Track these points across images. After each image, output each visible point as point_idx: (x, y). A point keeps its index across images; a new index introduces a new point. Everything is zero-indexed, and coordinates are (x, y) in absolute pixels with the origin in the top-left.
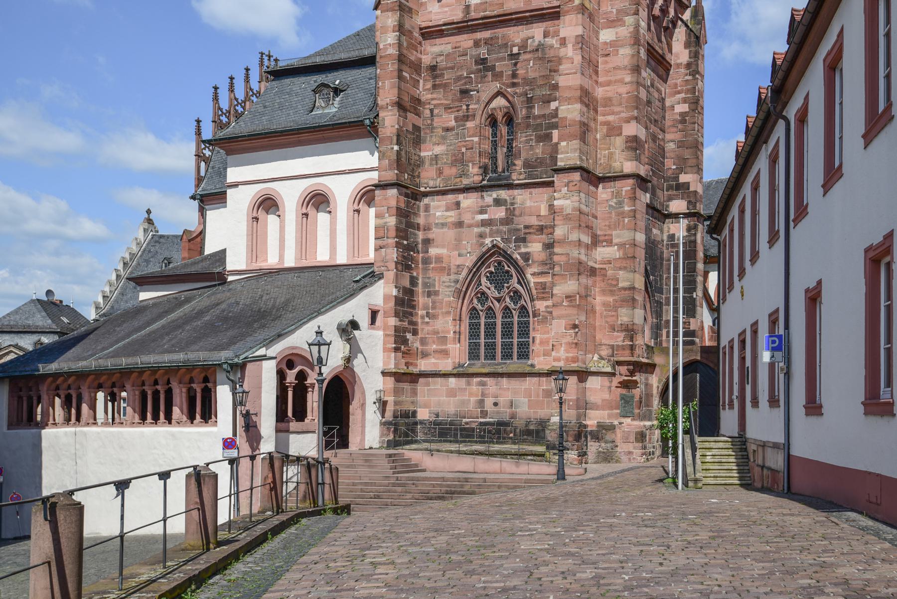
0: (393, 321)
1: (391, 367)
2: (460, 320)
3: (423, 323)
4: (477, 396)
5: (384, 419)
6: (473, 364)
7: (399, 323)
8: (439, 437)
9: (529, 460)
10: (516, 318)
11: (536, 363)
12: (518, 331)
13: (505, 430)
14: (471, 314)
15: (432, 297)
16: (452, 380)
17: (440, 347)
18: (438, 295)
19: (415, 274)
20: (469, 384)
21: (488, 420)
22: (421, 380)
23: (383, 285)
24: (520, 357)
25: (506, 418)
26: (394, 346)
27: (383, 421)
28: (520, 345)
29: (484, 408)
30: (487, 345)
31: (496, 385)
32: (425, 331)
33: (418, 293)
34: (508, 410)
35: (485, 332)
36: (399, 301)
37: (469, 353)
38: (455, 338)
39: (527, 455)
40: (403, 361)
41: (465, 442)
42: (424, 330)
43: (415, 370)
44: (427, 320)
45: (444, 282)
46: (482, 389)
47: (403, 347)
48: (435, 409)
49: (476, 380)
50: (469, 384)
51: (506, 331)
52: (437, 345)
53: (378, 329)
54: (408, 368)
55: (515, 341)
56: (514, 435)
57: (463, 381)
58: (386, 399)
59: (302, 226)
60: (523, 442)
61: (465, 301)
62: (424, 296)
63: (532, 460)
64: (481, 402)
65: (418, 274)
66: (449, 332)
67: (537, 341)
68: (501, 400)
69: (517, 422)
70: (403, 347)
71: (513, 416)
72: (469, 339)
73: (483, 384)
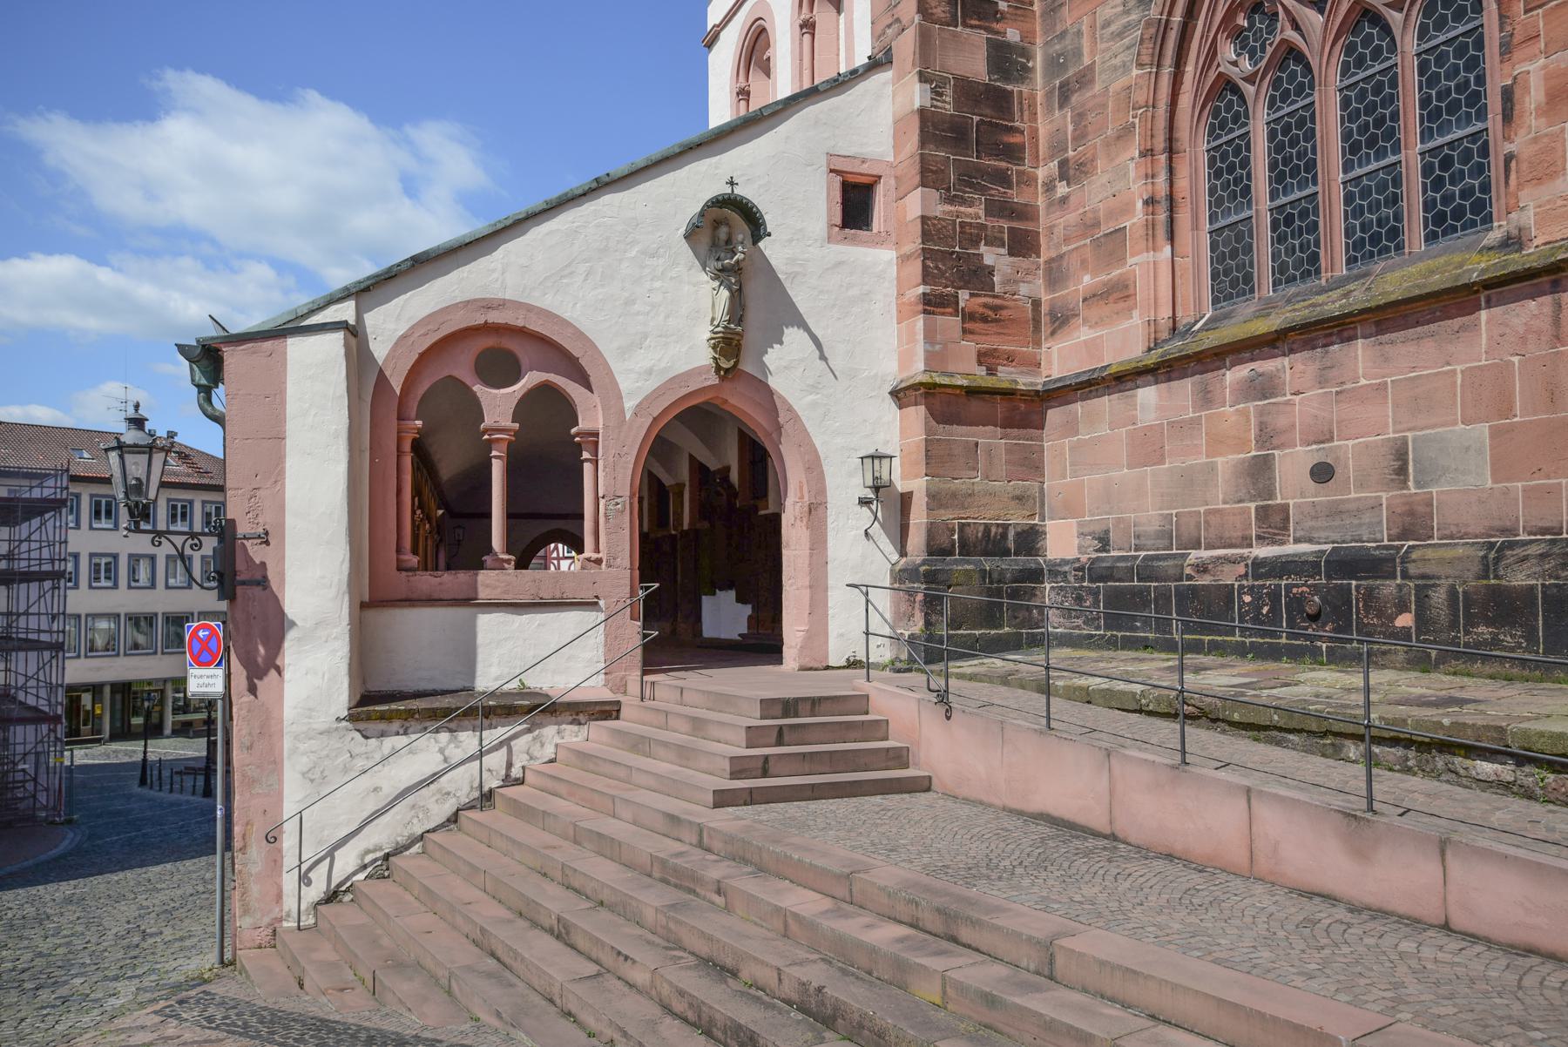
0: (915, 204)
1: (917, 370)
2: (1171, 150)
3: (1050, 205)
4: (1242, 445)
5: (904, 560)
6: (1227, 316)
7: (940, 210)
8: (1107, 628)
9: (1485, 784)
10: (1410, 44)
11: (1528, 218)
12: (1425, 102)
13: (1369, 596)
14: (1216, 113)
15: (1075, 99)
16: (1148, 395)
17: (1104, 277)
18: (1092, 81)
19: (1013, 35)
20: (1206, 398)
21: (1290, 549)
22: (1054, 416)
23: (890, 89)
24: (1441, 223)
25: (1376, 535)
26: (921, 289)
27: (898, 568)
28: (1439, 167)
29: (1271, 496)
30: (1284, 221)
31: (1322, 382)
32: (1059, 232)
33: (1032, 105)
34: (1384, 496)
35: (1273, 166)
36: (932, 128)
37: (1215, 276)
38: (1151, 226)
39: (1471, 751)
40: (970, 347)
41: (1196, 648)
42: (1053, 227)
43: (1024, 381)
44: (1062, 189)
45: (1107, 24)
46: (1261, 412)
47: (964, 295)
48: (1096, 519)
49: (1236, 375)
50: (1206, 398)
51: (1364, 129)
52: (1094, 274)
53: (878, 242)
54: (991, 371)
55: (1412, 155)
56: (1421, 619)
57: (1185, 388)
58: (901, 486)
59: (801, 60)
60: (1472, 658)
61: (1189, 68)
62: (1049, 110)
63: (1506, 787)
64: (1259, 472)
65: (1028, 36)
66: (1127, 209)
67: (1533, 97)
68: (1347, 451)
69: (1430, 553)
70: (964, 295)
71: (1413, 524)
72: (1213, 218)
73: (1263, 388)
